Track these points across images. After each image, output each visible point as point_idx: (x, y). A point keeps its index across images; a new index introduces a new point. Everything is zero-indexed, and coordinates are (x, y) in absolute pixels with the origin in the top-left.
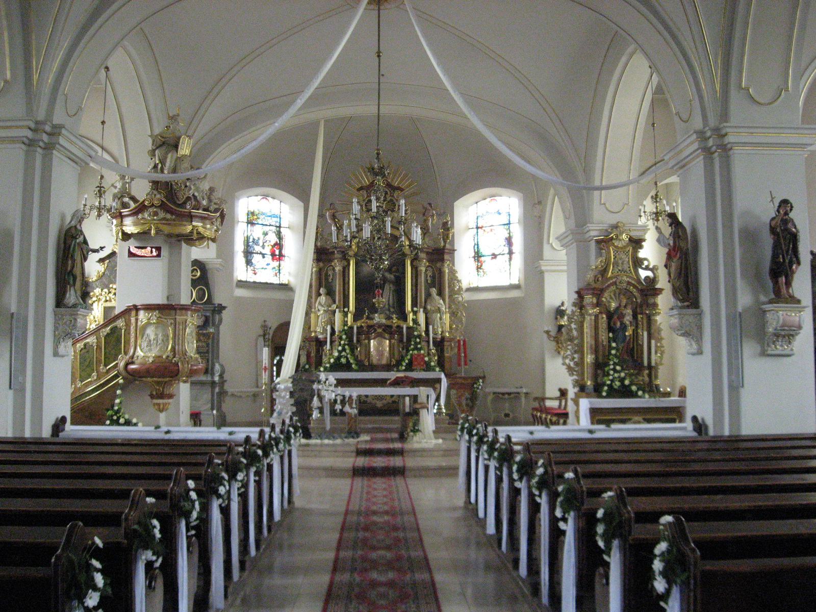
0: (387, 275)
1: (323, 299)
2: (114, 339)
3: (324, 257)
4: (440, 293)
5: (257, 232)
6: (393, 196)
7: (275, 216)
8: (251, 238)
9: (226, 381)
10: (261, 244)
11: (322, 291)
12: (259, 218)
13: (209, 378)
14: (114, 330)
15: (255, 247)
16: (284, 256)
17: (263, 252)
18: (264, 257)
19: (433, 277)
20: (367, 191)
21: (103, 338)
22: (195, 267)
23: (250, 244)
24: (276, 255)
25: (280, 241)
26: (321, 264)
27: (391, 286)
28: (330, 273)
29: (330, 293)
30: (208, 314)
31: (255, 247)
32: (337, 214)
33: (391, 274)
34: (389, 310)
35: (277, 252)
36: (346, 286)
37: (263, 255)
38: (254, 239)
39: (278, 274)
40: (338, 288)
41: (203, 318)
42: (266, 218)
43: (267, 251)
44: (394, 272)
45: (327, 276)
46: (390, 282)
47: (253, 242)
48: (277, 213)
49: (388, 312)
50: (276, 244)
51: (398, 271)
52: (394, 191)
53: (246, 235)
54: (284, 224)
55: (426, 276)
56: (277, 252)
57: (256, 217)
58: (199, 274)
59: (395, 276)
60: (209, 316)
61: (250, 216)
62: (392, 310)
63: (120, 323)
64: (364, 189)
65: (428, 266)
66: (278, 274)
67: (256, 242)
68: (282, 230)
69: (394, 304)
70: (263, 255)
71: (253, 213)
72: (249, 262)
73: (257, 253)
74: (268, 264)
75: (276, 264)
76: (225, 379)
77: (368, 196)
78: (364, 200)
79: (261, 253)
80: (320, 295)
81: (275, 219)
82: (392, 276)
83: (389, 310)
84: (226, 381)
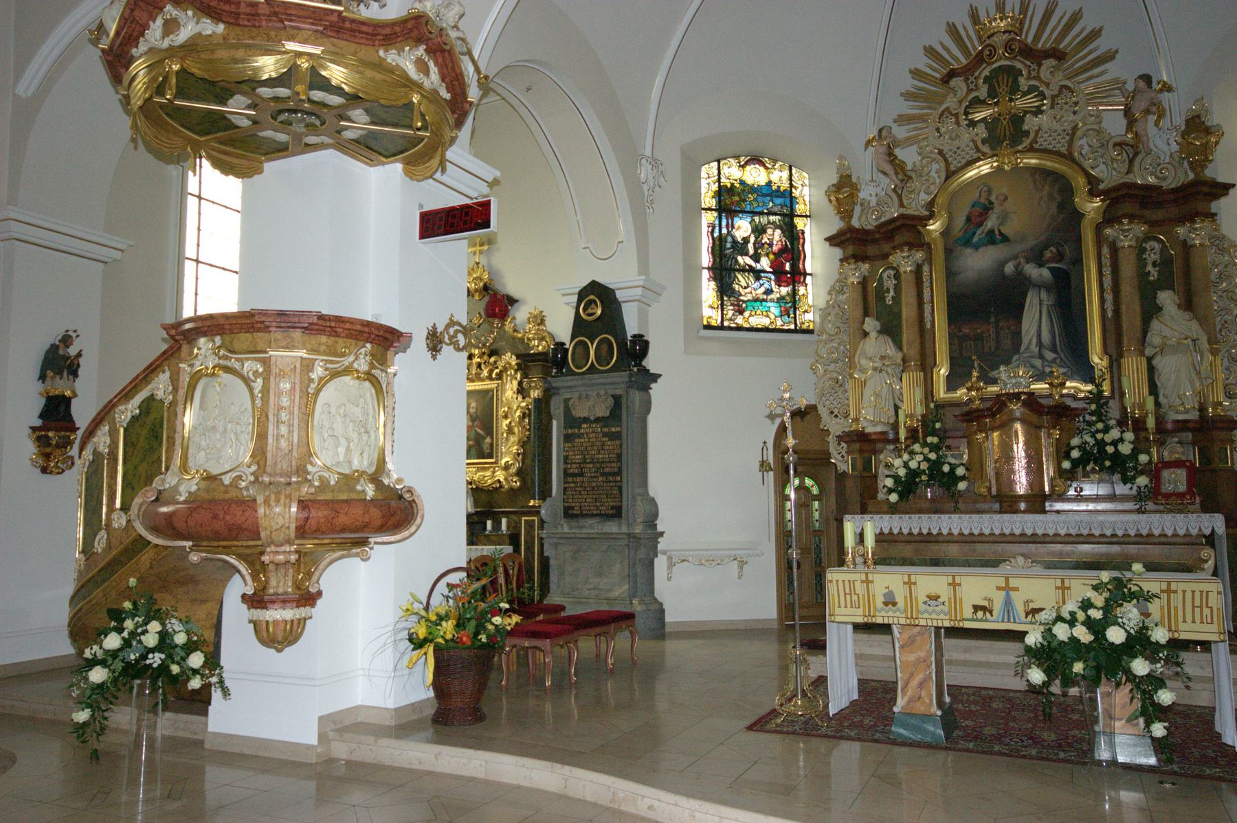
0: (1032, 270)
1: (876, 346)
2: (145, 433)
3: (871, 250)
4: (1188, 304)
5: (743, 228)
6: (1037, 78)
7: (778, 193)
8: (729, 239)
9: (662, 534)
10: (751, 252)
11: (871, 324)
12: (744, 201)
13: (624, 529)
14: (149, 404)
15: (740, 259)
16: (805, 274)
17: (758, 267)
18: (758, 278)
19: (1165, 263)
20: (967, 80)
21: (122, 430)
22: (592, 297)
23: (728, 252)
24: (787, 272)
25: (792, 244)
26: (865, 267)
27: (1044, 295)
28: (890, 283)
29: (891, 329)
30: (618, 392)
31: (740, 259)
32: (897, 152)
33: (1041, 266)
34: (1041, 357)
35: (788, 267)
36: (927, 308)
37: (758, 274)
38: (735, 242)
39: (791, 312)
40: (908, 312)
41: (611, 401)
42: (760, 199)
43: (765, 263)
44: (1052, 260)
45: (881, 293)
46: (1038, 286)
47: (732, 247)
48: (785, 185)
49: (1038, 363)
50: (784, 250)
51: (1060, 257)
52: (1040, 65)
53: (716, 234)
54: (800, 208)
55: (1142, 263)
56: (788, 267)
57: (737, 198)
58: (599, 312)
59: (1050, 269)
60: (620, 396)
61: (725, 196)
62: (1050, 355)
63: (161, 386)
64: (958, 75)
65: (1147, 238)
66: (791, 312)
67: (741, 247)
68: (796, 220)
69: (1054, 345)
70: (758, 274)
71: (731, 190)
72: (725, 289)
73: (743, 270)
74: (769, 292)
75: (784, 290)
76: (660, 529)
77: (970, 91)
78: (960, 102)
79: (751, 270)
80: (866, 334)
81: (778, 201)
82: (1045, 273)
83: (1041, 357)
84: (662, 534)
